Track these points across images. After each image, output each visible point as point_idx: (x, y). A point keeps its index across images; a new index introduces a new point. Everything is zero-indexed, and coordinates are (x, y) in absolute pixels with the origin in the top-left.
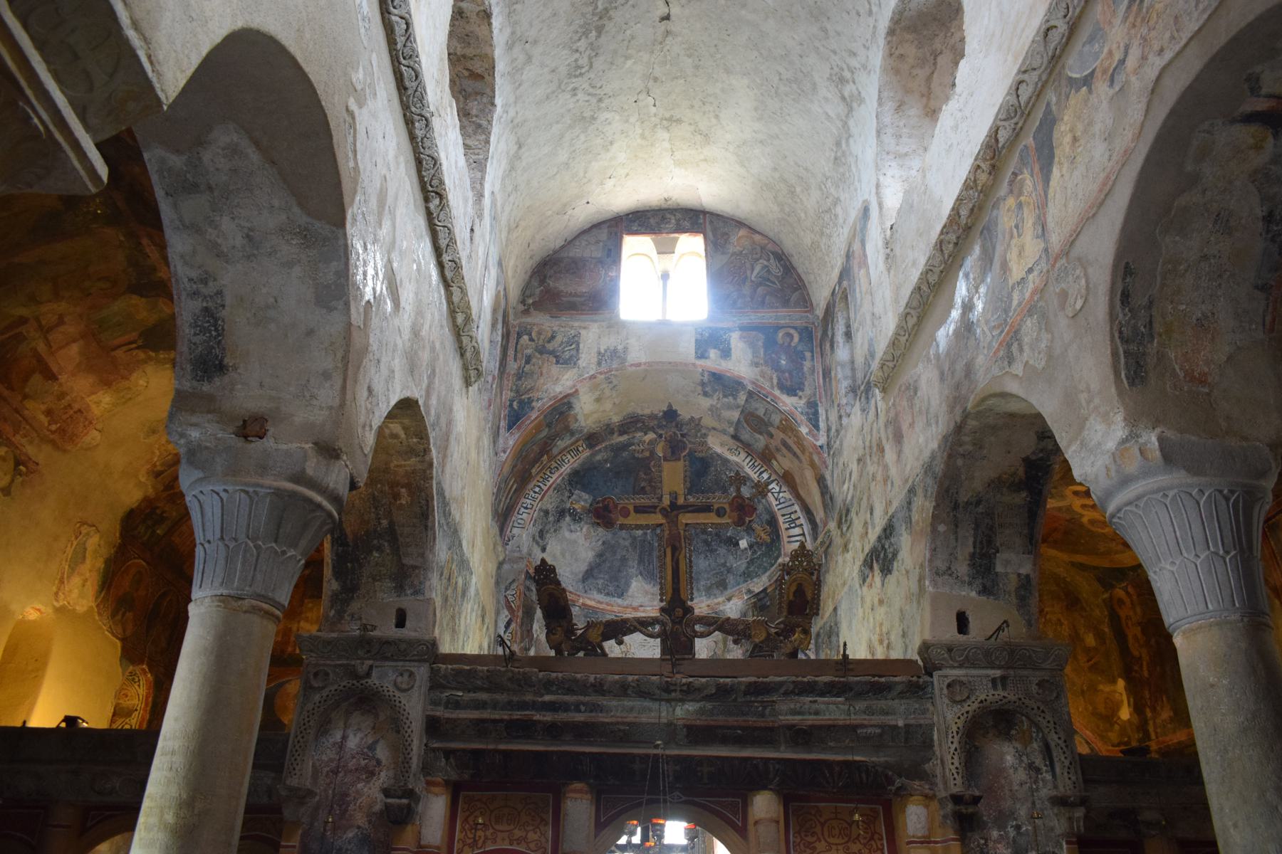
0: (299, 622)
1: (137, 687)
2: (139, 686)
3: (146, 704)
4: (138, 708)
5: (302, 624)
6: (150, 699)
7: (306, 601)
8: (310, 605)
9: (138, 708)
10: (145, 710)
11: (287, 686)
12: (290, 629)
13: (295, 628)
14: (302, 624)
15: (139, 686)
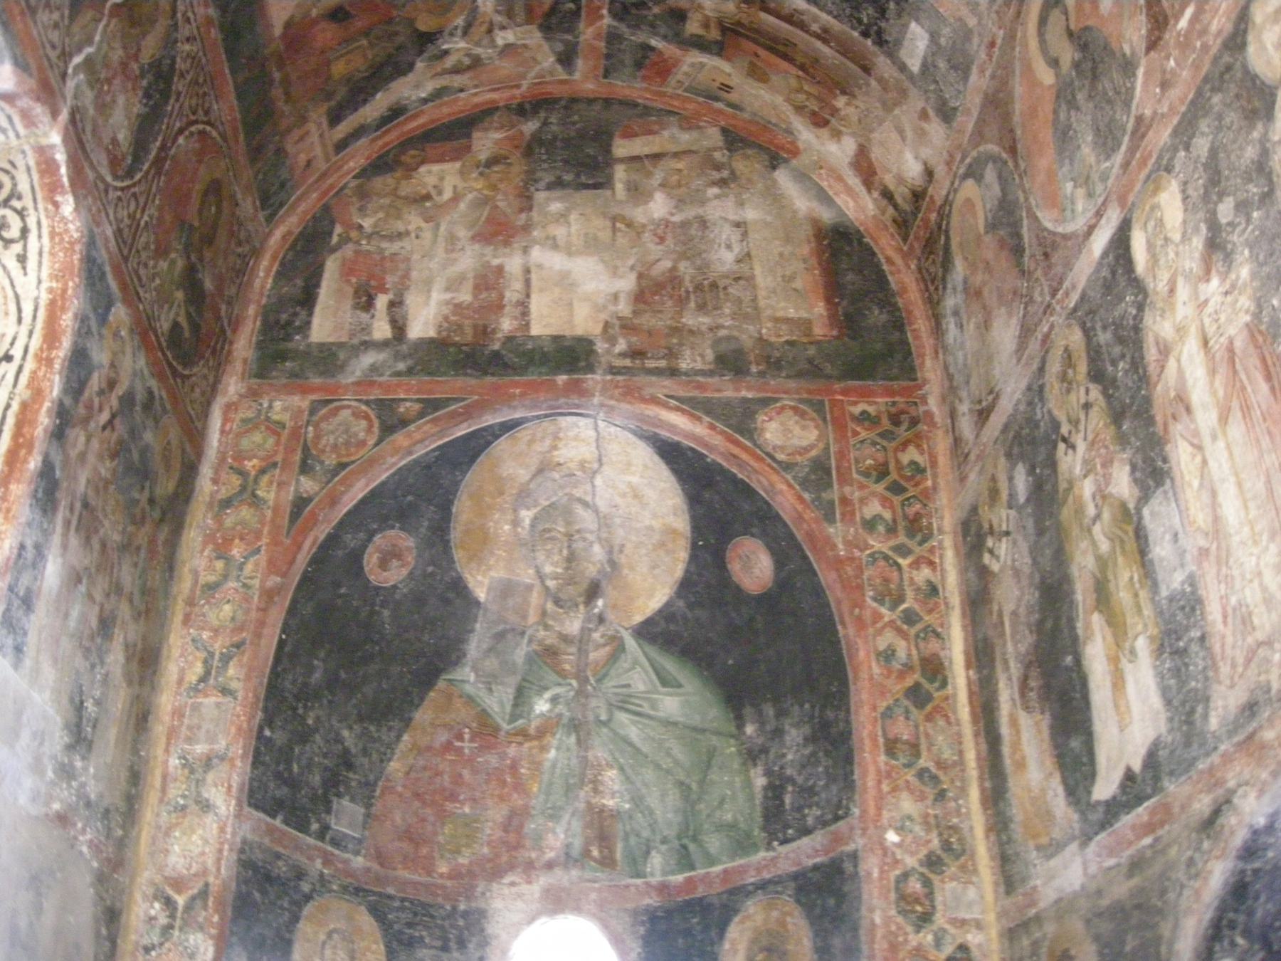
0: (526, 250)
1: (13, 265)
2: (22, 259)
3: (51, 337)
4: (17, 352)
5: (537, 254)
6: (67, 320)
7: (541, 196)
8: (556, 207)
9: (17, 352)
10: (44, 360)
11: (502, 445)
12: (500, 270)
13: (513, 264)
14: (537, 254)
15: (22, 259)
